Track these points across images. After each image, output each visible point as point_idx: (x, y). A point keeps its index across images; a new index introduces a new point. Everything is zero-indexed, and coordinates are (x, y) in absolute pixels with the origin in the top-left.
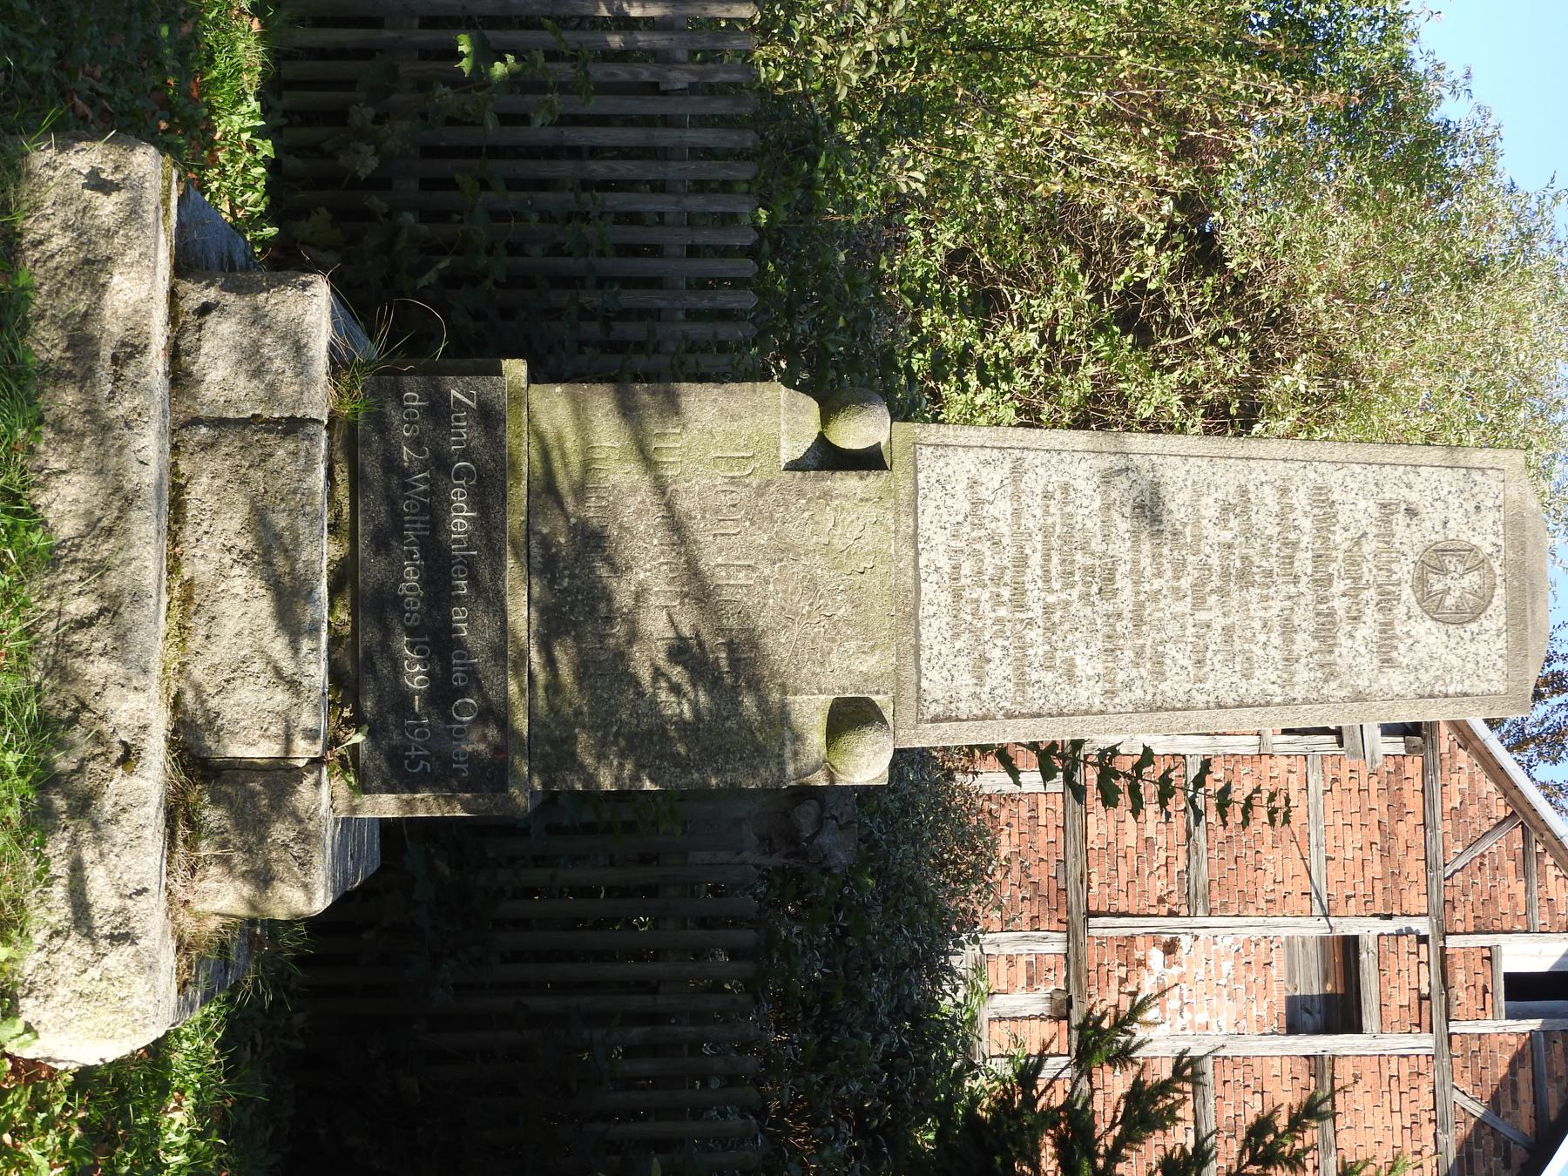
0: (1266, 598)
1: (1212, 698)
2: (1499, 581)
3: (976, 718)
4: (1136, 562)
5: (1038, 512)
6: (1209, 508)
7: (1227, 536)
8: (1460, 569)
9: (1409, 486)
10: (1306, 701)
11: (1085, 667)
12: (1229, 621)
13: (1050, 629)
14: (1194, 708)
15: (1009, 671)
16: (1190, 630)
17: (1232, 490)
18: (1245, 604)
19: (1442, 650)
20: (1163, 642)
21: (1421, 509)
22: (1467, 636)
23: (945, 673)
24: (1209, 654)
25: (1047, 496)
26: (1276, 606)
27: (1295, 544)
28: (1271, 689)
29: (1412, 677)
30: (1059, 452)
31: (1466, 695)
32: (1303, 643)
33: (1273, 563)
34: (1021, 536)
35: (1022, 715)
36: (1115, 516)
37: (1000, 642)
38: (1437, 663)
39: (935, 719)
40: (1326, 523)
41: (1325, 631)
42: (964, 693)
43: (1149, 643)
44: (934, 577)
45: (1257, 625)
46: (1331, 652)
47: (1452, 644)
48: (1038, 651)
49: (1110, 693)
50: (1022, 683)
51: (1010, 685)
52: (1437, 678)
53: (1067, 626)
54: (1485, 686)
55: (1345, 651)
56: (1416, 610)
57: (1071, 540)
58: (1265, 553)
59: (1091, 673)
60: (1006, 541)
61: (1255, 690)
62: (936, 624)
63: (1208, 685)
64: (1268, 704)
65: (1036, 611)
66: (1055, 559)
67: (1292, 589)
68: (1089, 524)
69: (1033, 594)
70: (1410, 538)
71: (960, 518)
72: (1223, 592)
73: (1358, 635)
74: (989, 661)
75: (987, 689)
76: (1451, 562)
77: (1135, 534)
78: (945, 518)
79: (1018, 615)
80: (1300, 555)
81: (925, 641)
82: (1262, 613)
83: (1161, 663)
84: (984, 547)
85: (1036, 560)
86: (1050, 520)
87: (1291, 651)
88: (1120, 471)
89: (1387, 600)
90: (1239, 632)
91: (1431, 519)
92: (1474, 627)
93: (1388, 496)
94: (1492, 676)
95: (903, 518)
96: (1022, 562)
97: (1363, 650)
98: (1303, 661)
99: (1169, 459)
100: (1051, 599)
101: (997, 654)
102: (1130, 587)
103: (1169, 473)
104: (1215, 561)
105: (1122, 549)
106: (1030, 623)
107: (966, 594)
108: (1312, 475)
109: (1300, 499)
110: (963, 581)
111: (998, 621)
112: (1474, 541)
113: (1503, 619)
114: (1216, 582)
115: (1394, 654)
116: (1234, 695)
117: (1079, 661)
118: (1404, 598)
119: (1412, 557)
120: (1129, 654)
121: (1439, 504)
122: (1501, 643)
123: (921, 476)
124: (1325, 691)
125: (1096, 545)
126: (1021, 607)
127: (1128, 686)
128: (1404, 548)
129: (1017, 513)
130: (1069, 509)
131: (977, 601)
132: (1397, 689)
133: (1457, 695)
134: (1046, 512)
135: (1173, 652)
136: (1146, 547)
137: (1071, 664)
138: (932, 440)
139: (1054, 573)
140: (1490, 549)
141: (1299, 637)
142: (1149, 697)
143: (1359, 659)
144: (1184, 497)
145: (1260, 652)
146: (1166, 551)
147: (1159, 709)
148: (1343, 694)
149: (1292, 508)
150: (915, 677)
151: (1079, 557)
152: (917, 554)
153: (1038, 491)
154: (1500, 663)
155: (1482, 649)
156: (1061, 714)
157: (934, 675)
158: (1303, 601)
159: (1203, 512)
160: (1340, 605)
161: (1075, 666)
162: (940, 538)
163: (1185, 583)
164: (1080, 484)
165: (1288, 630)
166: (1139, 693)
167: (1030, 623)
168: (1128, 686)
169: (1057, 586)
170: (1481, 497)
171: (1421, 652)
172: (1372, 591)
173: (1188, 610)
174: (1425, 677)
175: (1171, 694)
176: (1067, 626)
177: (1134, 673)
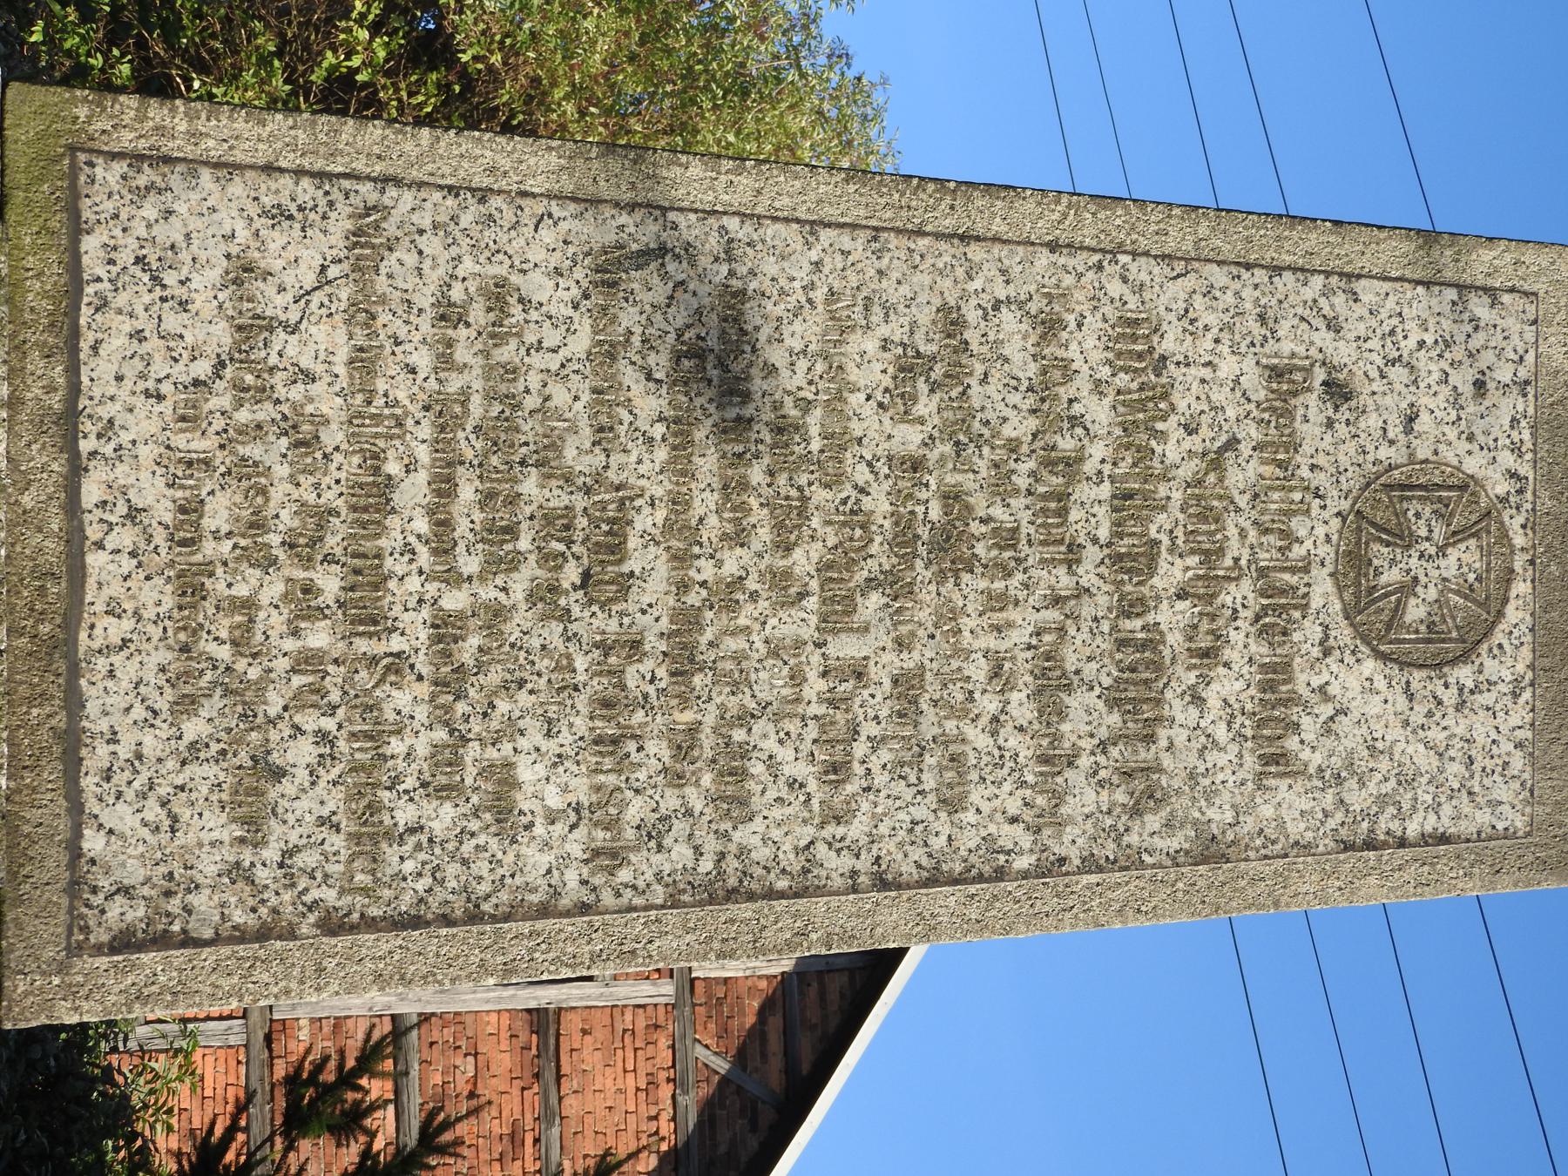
0: (997, 602)
1: (864, 864)
2: (1519, 563)
3: (241, 936)
4: (679, 502)
5: (423, 360)
6: (869, 368)
7: (910, 438)
8: (1439, 532)
9: (1334, 326)
10: (1090, 864)
11: (542, 786)
12: (910, 661)
13: (451, 683)
14: (820, 891)
15: (335, 801)
16: (815, 685)
17: (925, 316)
18: (949, 616)
19: (1396, 733)
20: (745, 718)
21: (1358, 382)
22: (1449, 697)
23: (153, 812)
24: (860, 748)
25: (449, 315)
26: (1024, 621)
27: (1071, 465)
28: (1010, 835)
29: (1329, 799)
30: (483, 194)
31: (1444, 839)
32: (1086, 715)
33: (1018, 512)
34: (373, 426)
35: (369, 924)
36: (630, 376)
37: (310, 721)
38: (1384, 765)
39: (124, 943)
40: (1144, 411)
41: (1137, 690)
42: (208, 866)
43: (710, 720)
44: (125, 537)
45: (978, 670)
46: (1150, 739)
47: (1417, 718)
48: (415, 746)
49: (608, 857)
50: (371, 834)
51: (337, 842)
52: (1382, 800)
53: (494, 677)
54: (1484, 818)
55: (1181, 736)
56: (1343, 634)
57: (514, 439)
58: (1001, 487)
59: (555, 800)
60: (333, 436)
61: (969, 840)
62: (128, 670)
63: (856, 830)
64: (1000, 874)
65: (412, 634)
66: (467, 492)
67: (1063, 580)
68: (560, 396)
69: (406, 586)
70: (1330, 450)
71: (202, 369)
72: (896, 586)
73: (1212, 696)
74: (279, 774)
75: (271, 853)
76: (1422, 519)
77: (680, 427)
78: (160, 367)
79: (362, 646)
80: (1084, 492)
81: (95, 721)
82: (991, 642)
83: (741, 775)
84: (272, 453)
85: (414, 491)
86: (455, 384)
87: (1056, 738)
88: (643, 257)
89: (1278, 610)
90: (932, 688)
91: (1381, 406)
92: (1463, 674)
93: (1287, 347)
94: (1503, 792)
95: (35, 362)
96: (374, 498)
97: (1221, 732)
98: (1085, 762)
99: (771, 230)
100: (455, 600)
101: (303, 752)
102: (662, 569)
103: (770, 267)
104: (879, 504)
105: (643, 466)
106: (397, 666)
107: (218, 586)
108: (1115, 288)
109: (1086, 347)
110: (209, 548)
111: (307, 661)
112: (1472, 465)
113: (1526, 654)
114: (880, 557)
115: (1292, 743)
116: (918, 854)
117: (527, 773)
118: (1316, 602)
119: (1337, 504)
120: (658, 749)
121: (1398, 374)
122: (1519, 715)
123: (91, 245)
124: (1133, 839)
125: (577, 455)
126: (372, 621)
127: (654, 835)
128: (1320, 479)
129: (363, 362)
130: (507, 353)
131: (248, 605)
132: (1296, 829)
133: (1426, 840)
134: (445, 361)
135: (771, 745)
136: (707, 464)
137: (503, 778)
138: (126, 140)
139: (462, 528)
140: (1501, 489)
141: (1076, 702)
142: (707, 865)
143: (1213, 757)
144: (805, 331)
145: (983, 741)
146: (757, 475)
147: (732, 895)
148: (1174, 844)
149: (1067, 371)
150: (63, 825)
151: (530, 486)
152: (76, 470)
153: (424, 300)
154: (1518, 762)
155: (1482, 728)
156: (474, 917)
157: (122, 817)
158: (1087, 610)
159: (854, 374)
160: (1172, 618)
161: (516, 785)
162: (143, 423)
163: (803, 560)
164: (538, 286)
165: (1052, 684)
166: (681, 854)
167: (397, 666)
168: (654, 835)
169: (470, 564)
170: (1488, 358)
171: (1351, 735)
172: (1246, 586)
173: (808, 633)
174: (1358, 799)
175: (762, 853)
176: (494, 677)
177: (671, 802)
